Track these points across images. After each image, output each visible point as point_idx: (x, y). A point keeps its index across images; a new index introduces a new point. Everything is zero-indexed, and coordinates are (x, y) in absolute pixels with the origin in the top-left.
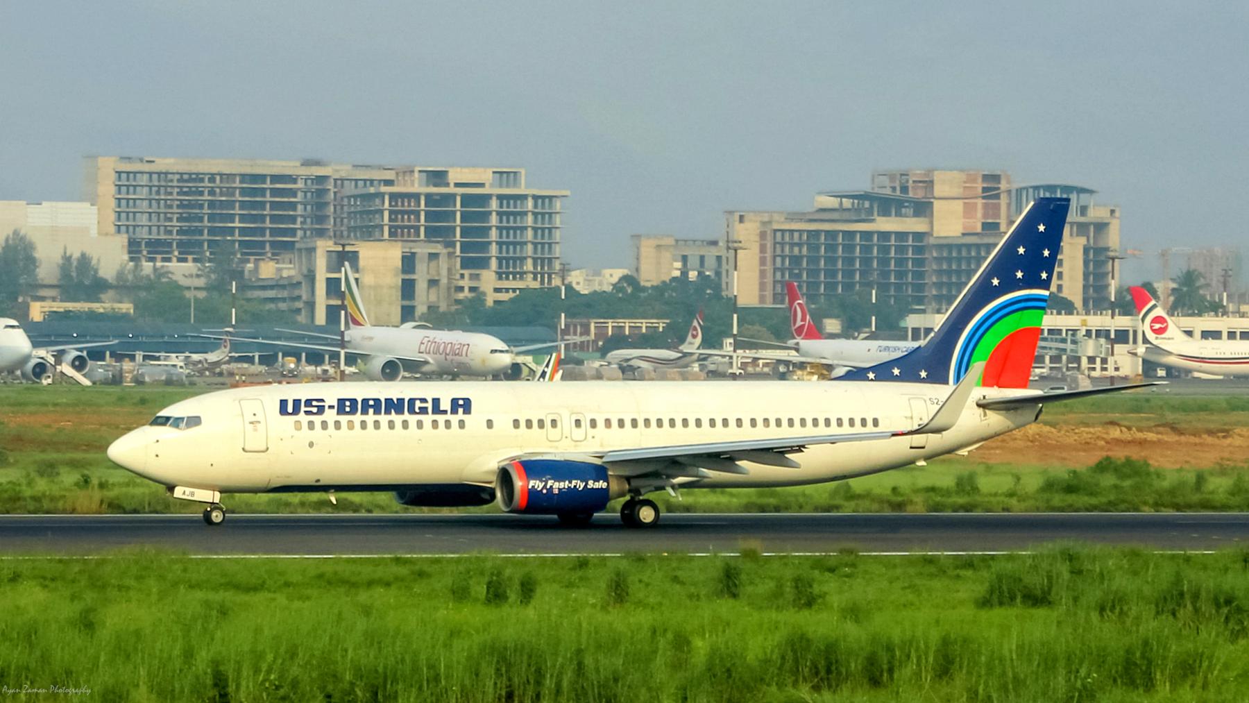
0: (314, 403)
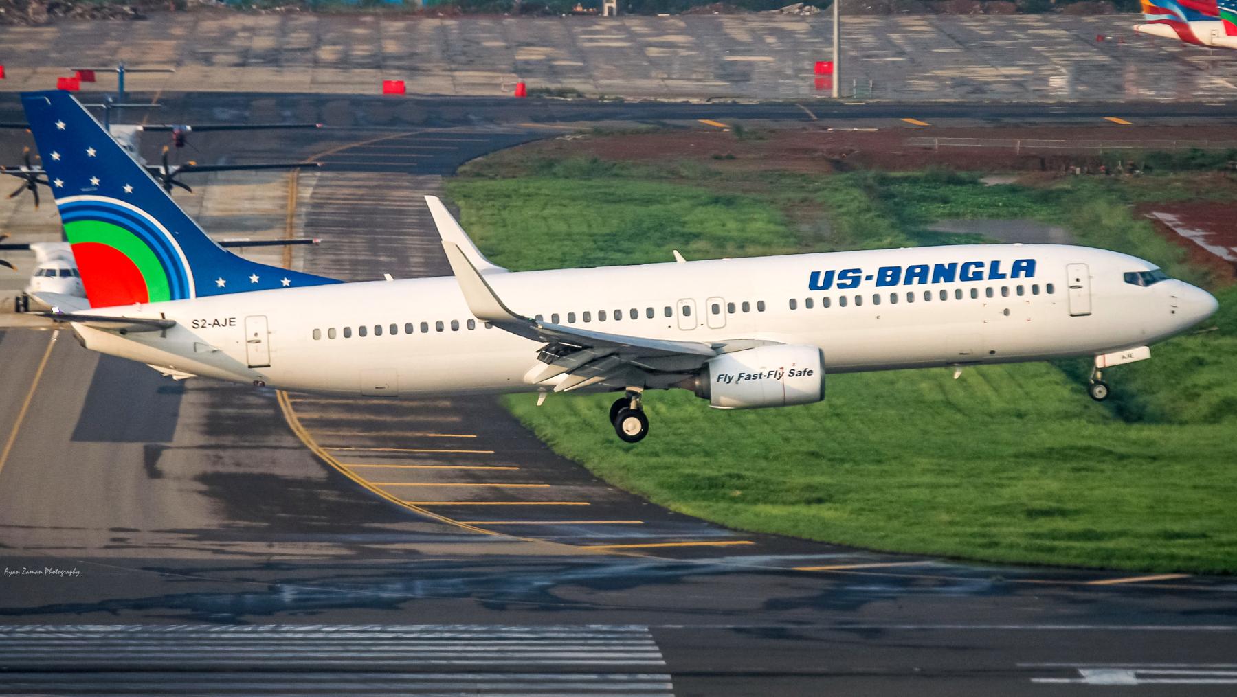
0: (850, 274)
